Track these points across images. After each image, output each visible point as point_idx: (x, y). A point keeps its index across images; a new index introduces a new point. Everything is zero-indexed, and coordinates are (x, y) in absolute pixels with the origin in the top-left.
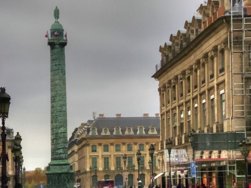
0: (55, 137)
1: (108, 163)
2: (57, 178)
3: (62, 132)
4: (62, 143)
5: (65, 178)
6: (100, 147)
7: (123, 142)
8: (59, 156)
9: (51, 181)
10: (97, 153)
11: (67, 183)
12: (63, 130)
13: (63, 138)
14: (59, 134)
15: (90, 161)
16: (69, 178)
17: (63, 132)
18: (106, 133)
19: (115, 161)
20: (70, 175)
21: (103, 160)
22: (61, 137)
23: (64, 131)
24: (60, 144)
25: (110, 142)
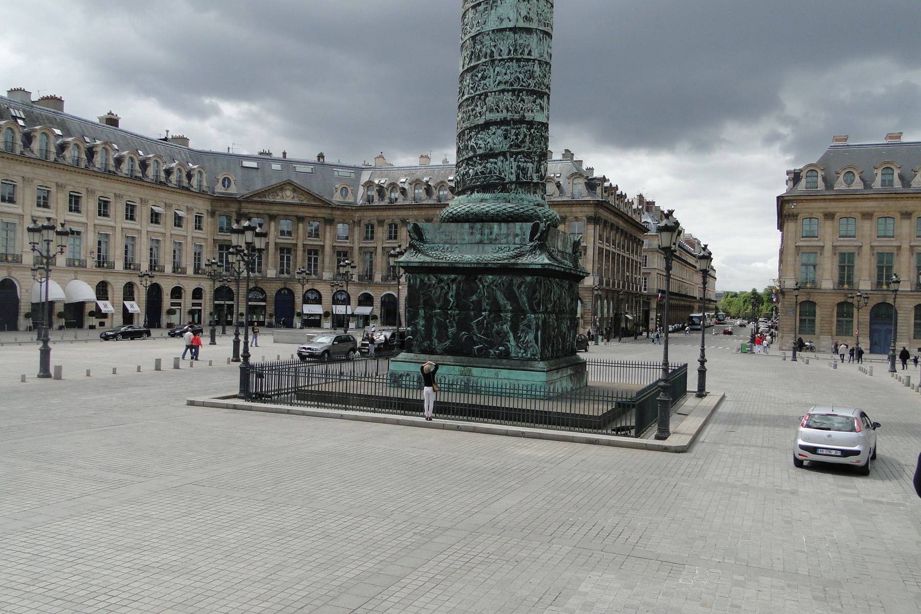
0: (467, 60)
1: (851, 268)
2: (457, 295)
3: (505, 30)
4: (503, 91)
5: (502, 300)
6: (829, 223)
7: (904, 210)
8: (479, 168)
9: (422, 312)
10: (819, 240)
11: (506, 327)
12: (513, 16)
13: (514, 63)
14: (487, 40)
15: (795, 260)
16: (525, 299)
17: (514, 30)
18: (849, 185)
19: (874, 266)
20: (528, 279)
21: (837, 259)
22: (497, 57)
23: (521, 24)
24: (490, 100)
25: (860, 210)
